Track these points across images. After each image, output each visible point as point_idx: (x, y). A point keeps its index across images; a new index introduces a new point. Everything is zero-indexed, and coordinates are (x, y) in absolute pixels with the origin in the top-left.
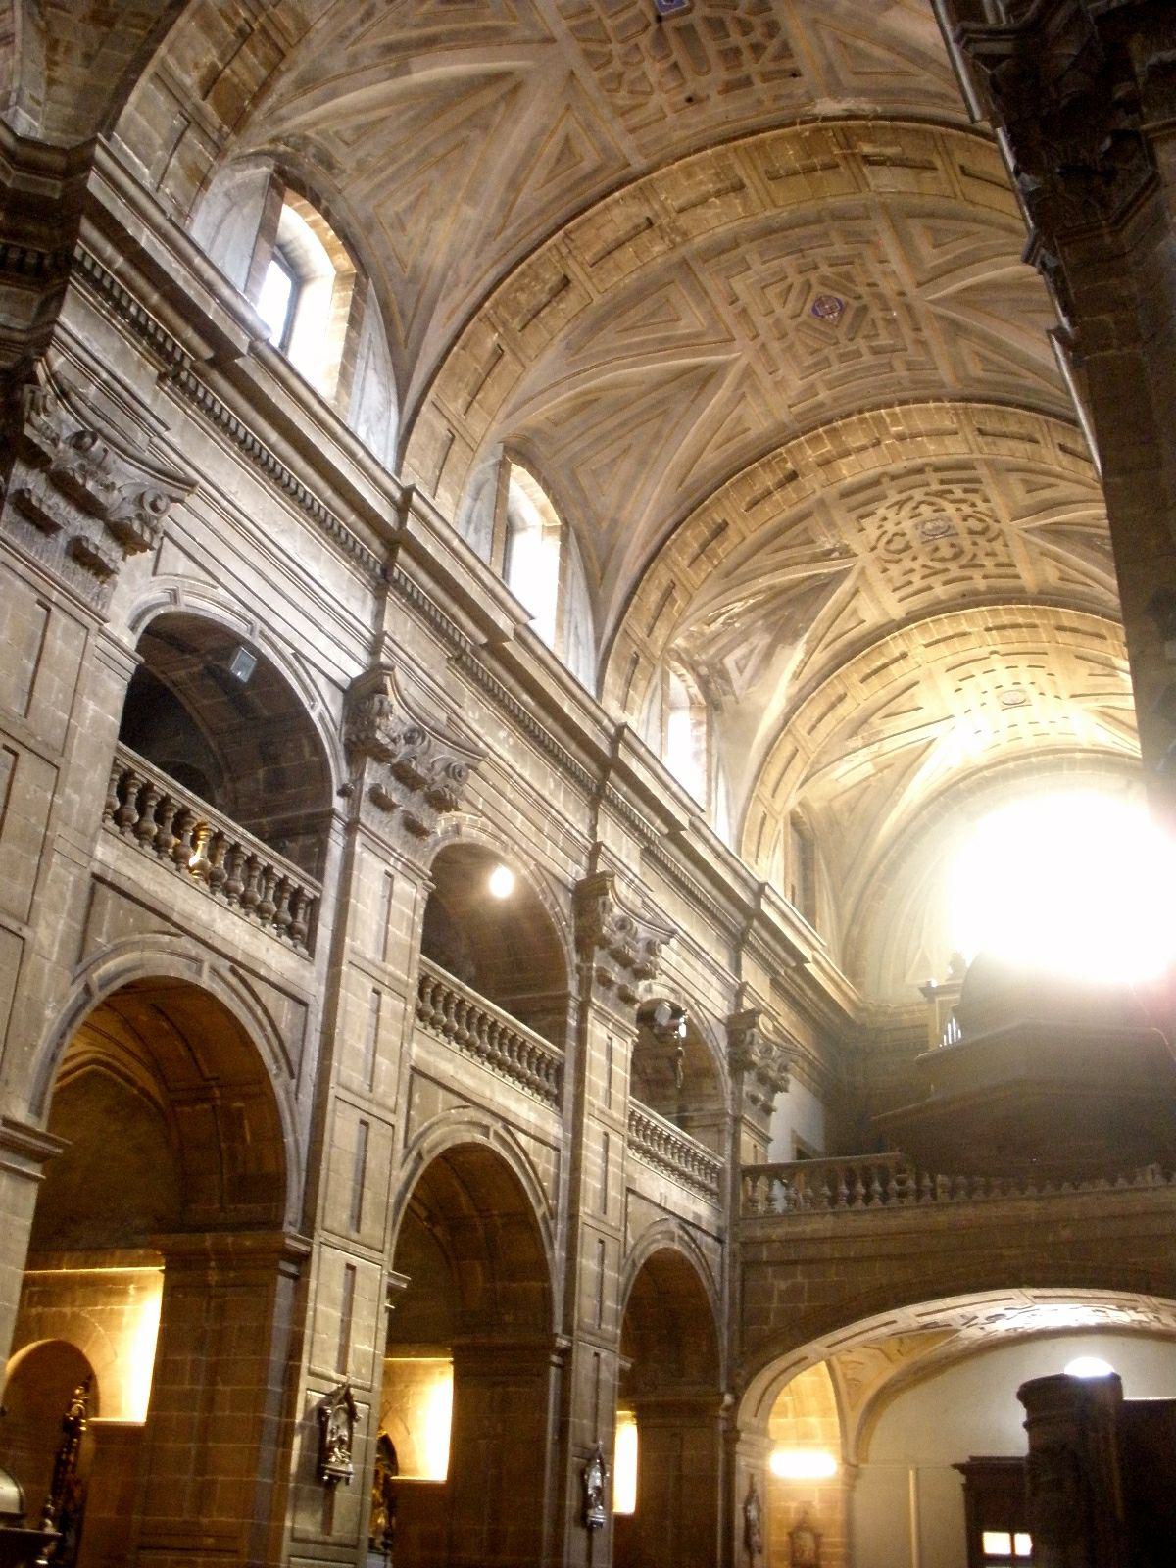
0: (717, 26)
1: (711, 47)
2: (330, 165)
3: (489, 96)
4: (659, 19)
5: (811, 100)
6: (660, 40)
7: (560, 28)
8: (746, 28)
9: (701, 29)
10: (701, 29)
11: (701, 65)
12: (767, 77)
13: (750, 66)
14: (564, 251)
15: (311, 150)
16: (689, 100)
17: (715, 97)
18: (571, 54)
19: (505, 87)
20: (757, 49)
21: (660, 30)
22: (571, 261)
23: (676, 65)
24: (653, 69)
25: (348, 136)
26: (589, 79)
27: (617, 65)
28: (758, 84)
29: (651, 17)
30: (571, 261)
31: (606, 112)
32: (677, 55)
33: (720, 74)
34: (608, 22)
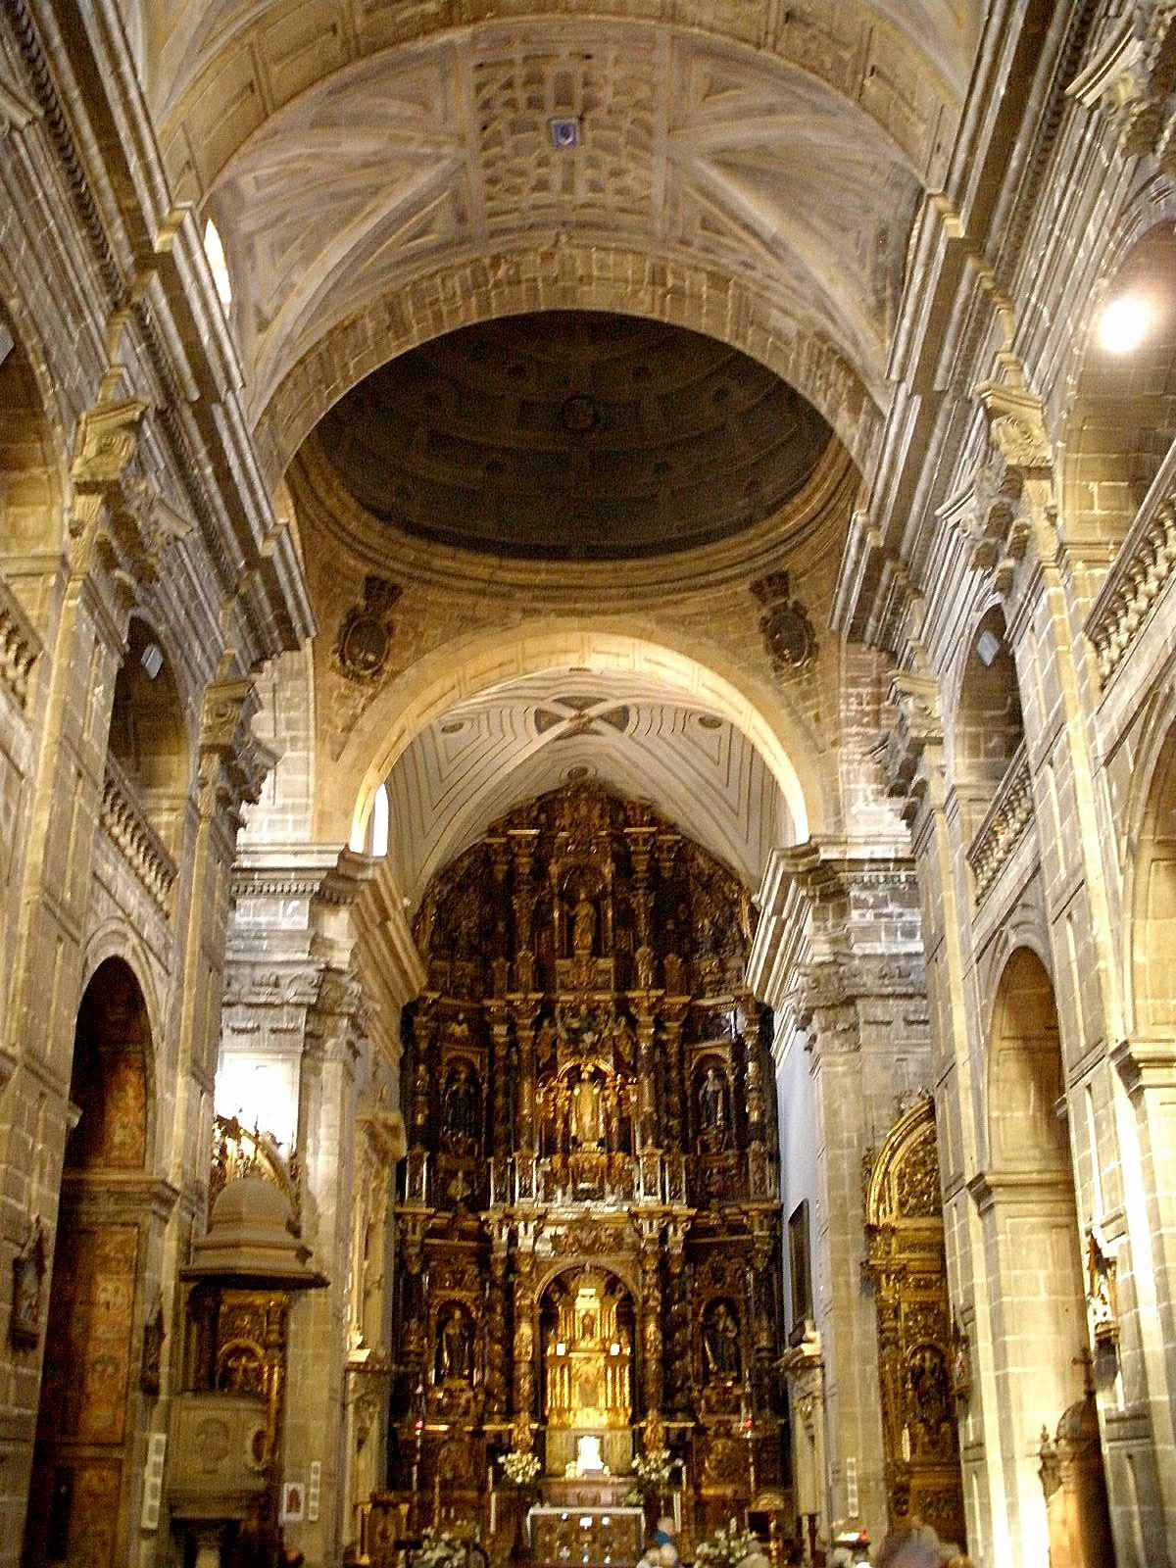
0: (535, 103)
1: (548, 92)
2: (882, 235)
3: (743, 159)
4: (581, 119)
5: (475, 38)
6: (590, 104)
7: (658, 161)
8: (511, 103)
9: (550, 103)
10: (550, 103)
11: (564, 79)
12: (511, 62)
13: (519, 73)
14: (770, 39)
15: (881, 258)
16: (588, 57)
17: (564, 52)
18: (660, 141)
19: (728, 157)
20: (509, 85)
21: (586, 109)
22: (772, 26)
23: (586, 84)
24: (606, 96)
25: (852, 235)
26: (659, 120)
27: (632, 114)
28: (518, 57)
29: (586, 124)
30: (772, 26)
31: (662, 90)
32: (579, 93)
33: (550, 71)
34: (622, 140)
